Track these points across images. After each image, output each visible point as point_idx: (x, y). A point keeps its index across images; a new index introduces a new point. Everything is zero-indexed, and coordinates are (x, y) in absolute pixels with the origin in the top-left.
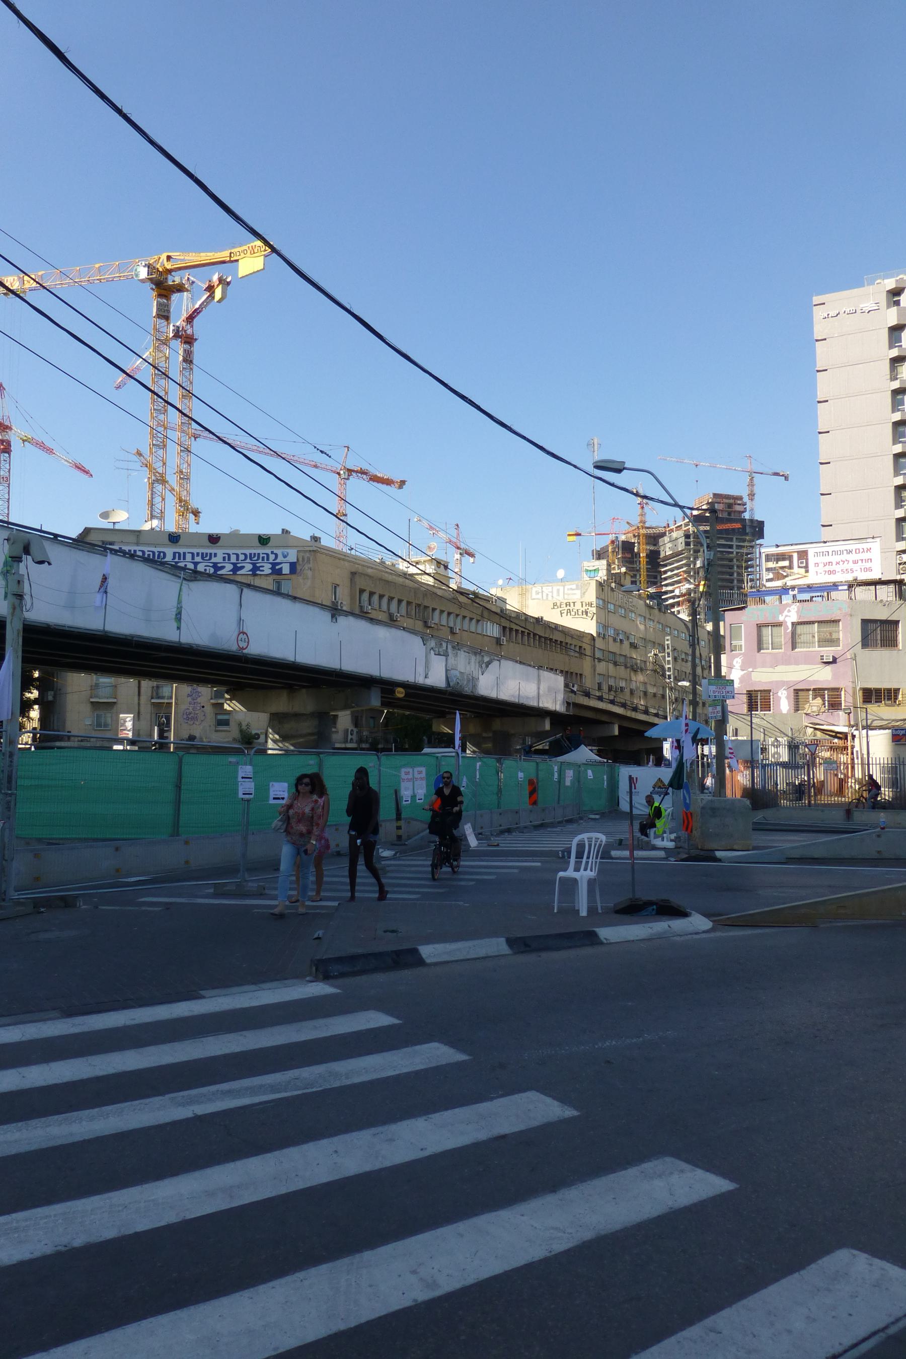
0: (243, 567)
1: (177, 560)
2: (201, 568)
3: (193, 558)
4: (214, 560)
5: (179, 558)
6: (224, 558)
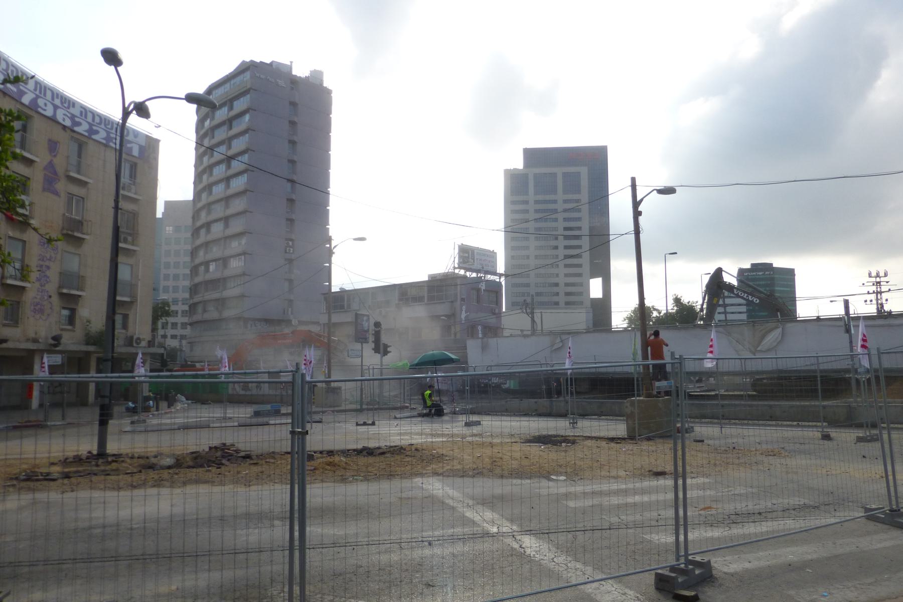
0: (97, 132)
1: (37, 92)
2: (60, 116)
3: (53, 99)
4: (72, 110)
5: (40, 92)
6: (81, 113)
